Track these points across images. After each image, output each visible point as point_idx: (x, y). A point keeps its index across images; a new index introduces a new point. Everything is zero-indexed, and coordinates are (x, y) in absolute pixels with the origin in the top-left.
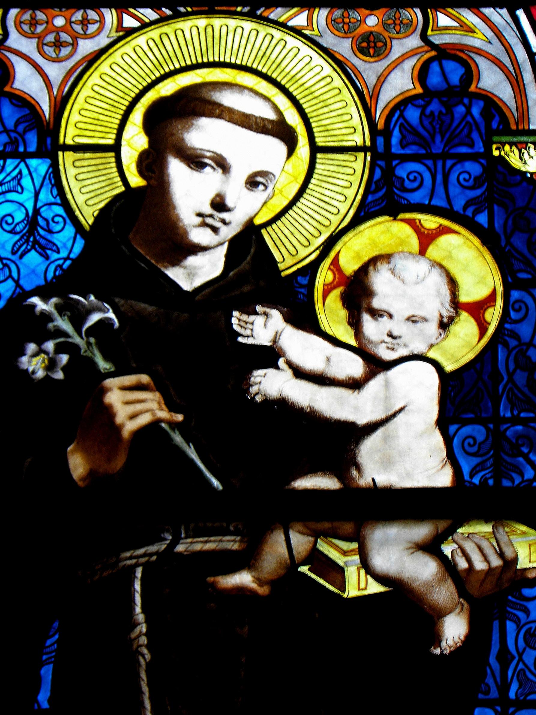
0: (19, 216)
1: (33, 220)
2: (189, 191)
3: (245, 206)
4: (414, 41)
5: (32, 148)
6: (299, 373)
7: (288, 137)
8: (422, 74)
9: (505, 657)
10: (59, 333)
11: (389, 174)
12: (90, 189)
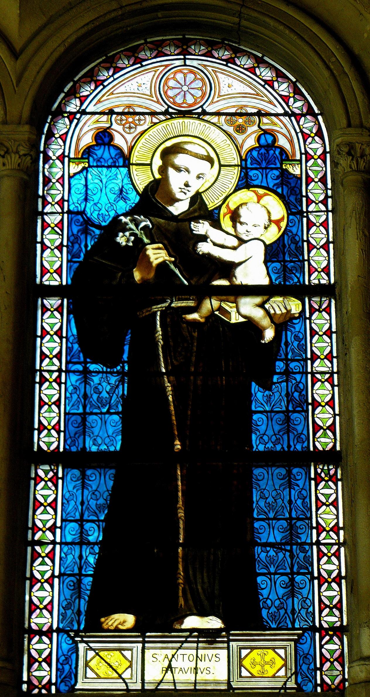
0: (117, 188)
1: (121, 191)
2: (176, 180)
3: (196, 186)
4: (256, 128)
5: (121, 164)
6: (215, 244)
7: (211, 161)
8: (259, 139)
9: (287, 344)
10: (131, 229)
11: (246, 174)
12: (142, 179)
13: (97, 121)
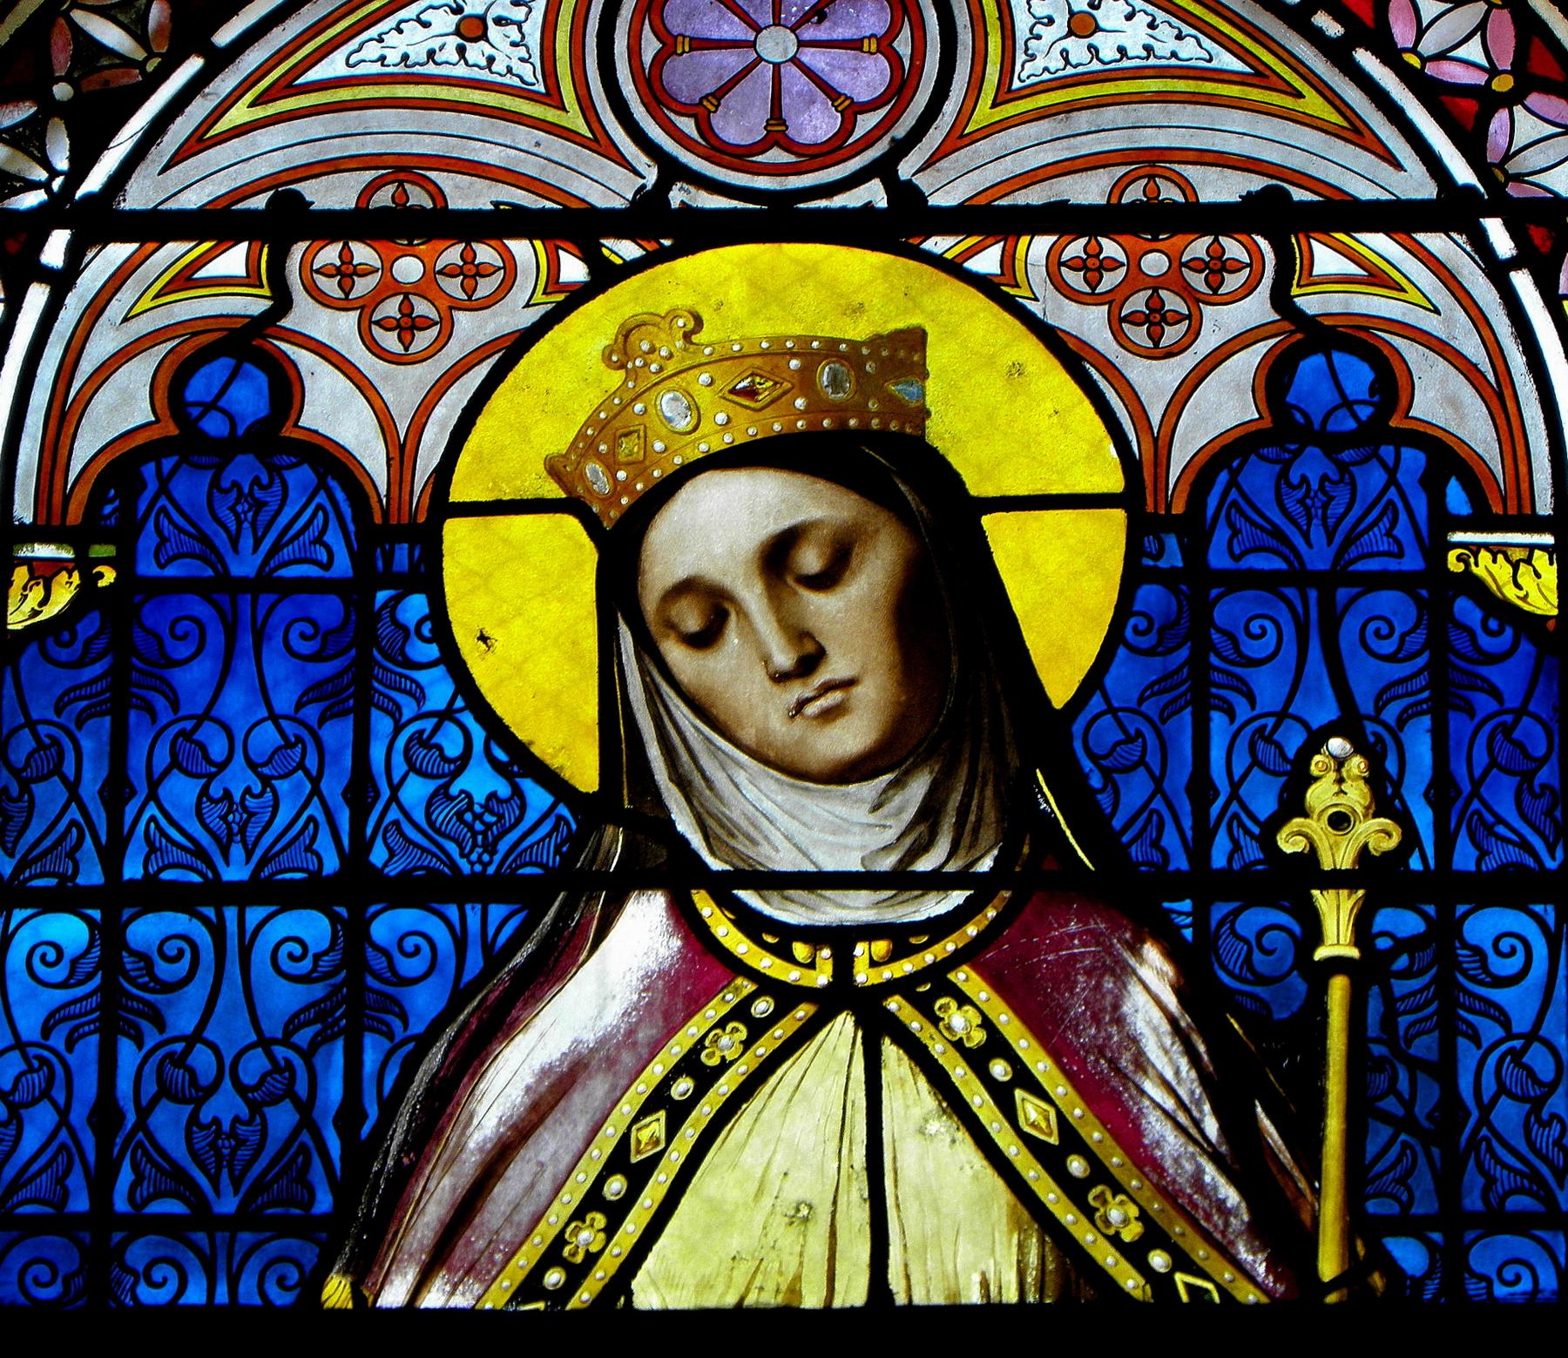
4: (1257, 309)
13: (185, 280)
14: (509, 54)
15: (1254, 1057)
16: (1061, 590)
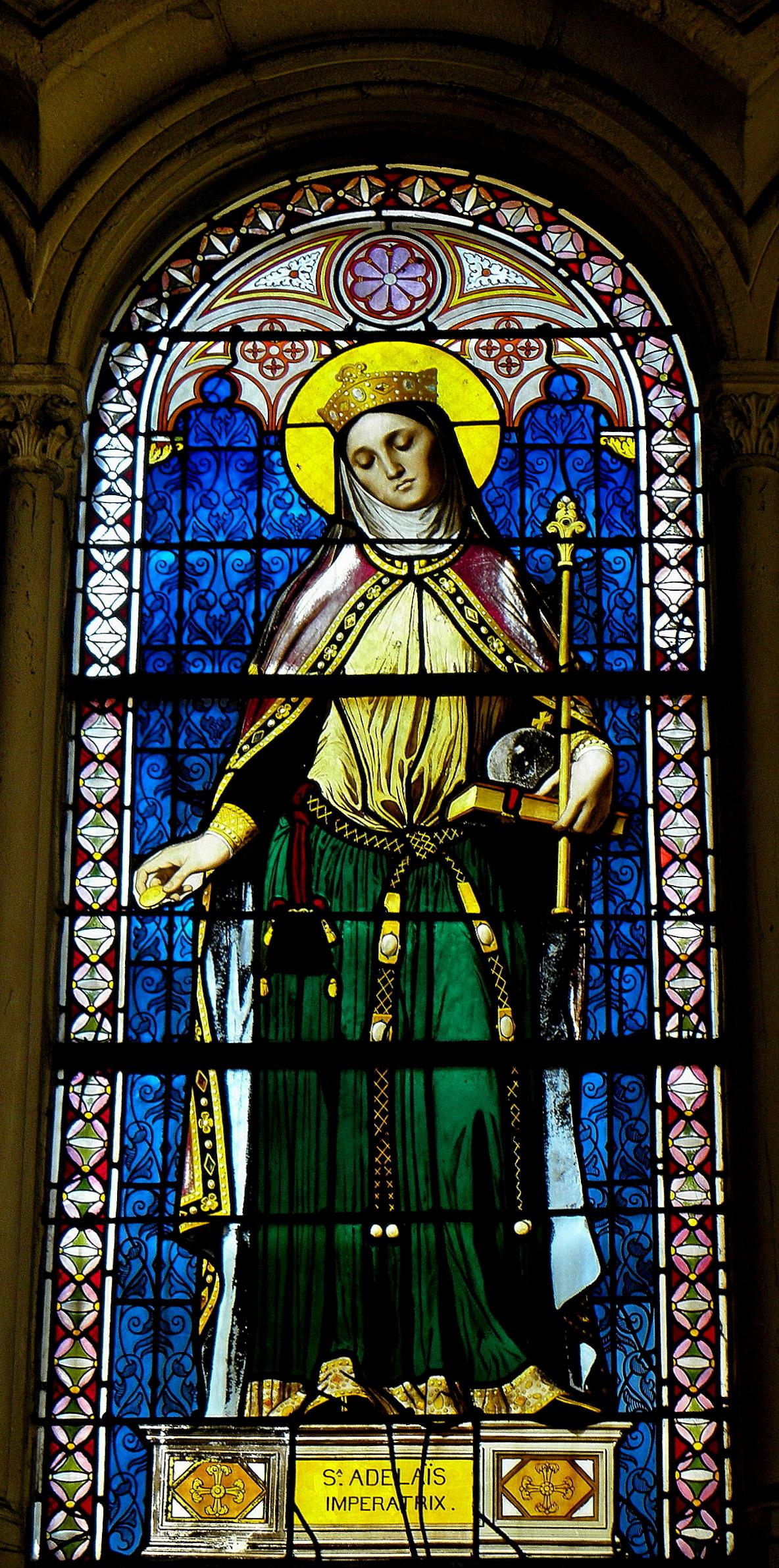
4: (541, 362)
8: (546, 384)
14: (306, 283)
15: (538, 595)
16: (480, 451)
